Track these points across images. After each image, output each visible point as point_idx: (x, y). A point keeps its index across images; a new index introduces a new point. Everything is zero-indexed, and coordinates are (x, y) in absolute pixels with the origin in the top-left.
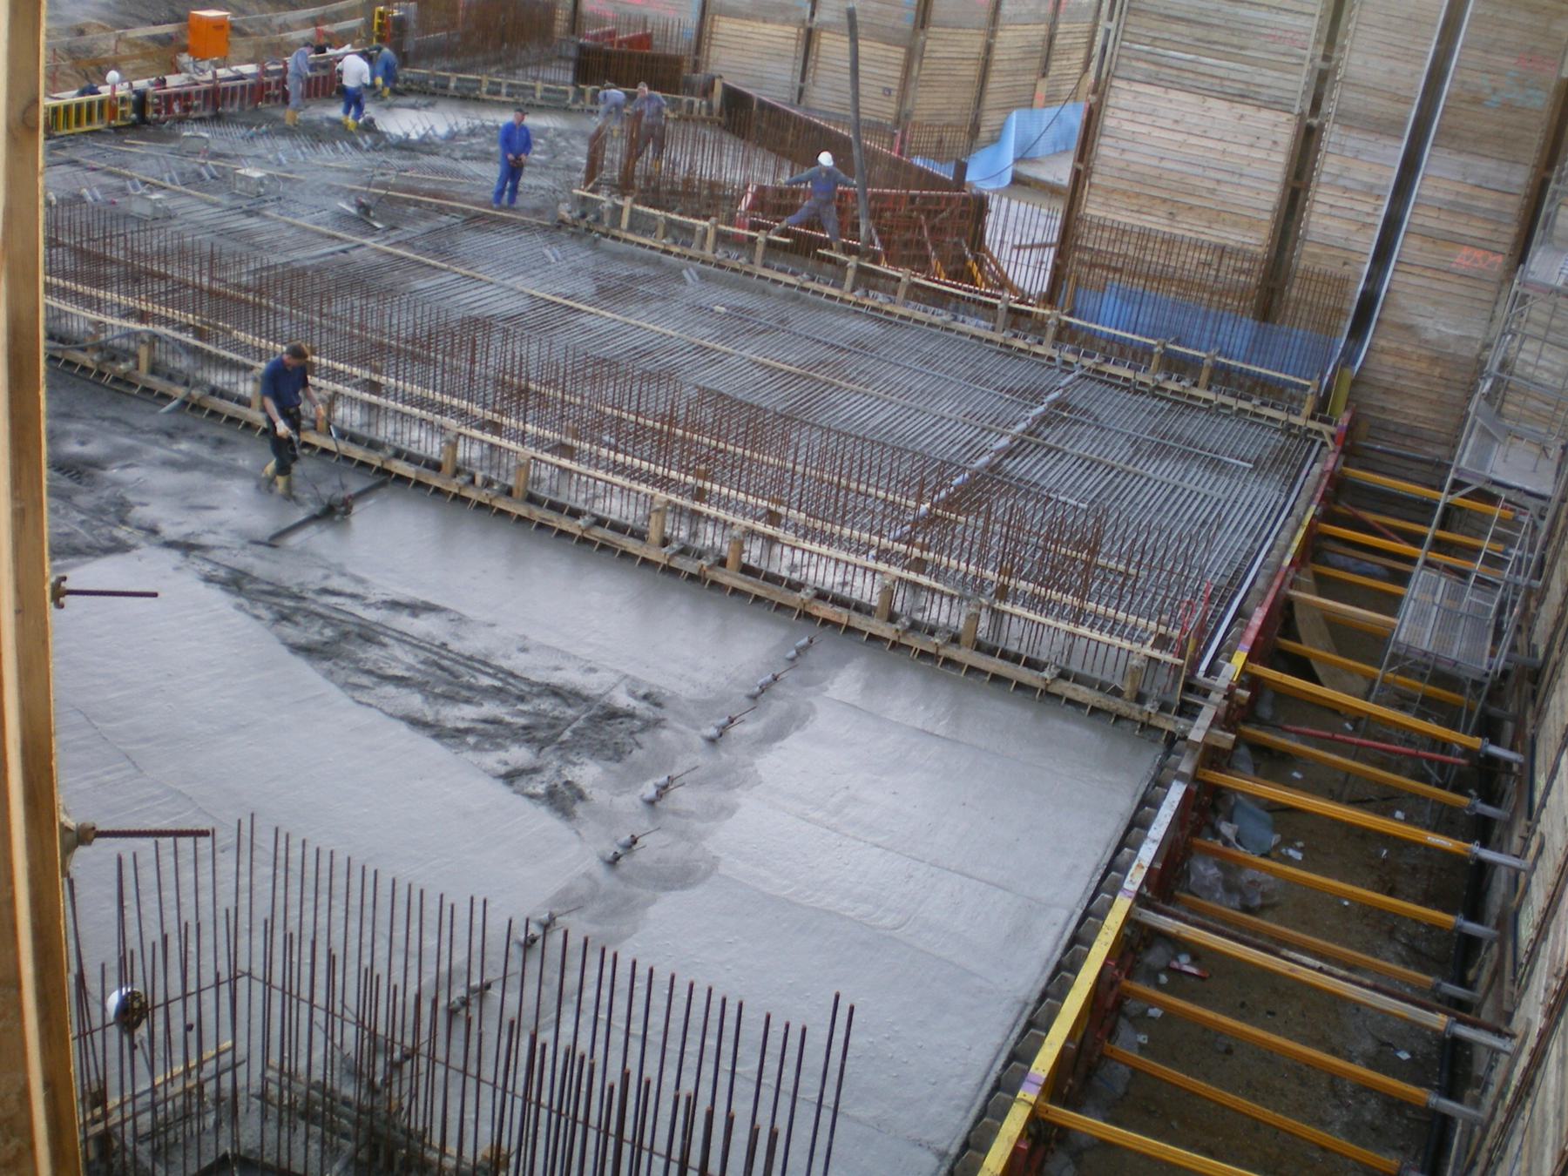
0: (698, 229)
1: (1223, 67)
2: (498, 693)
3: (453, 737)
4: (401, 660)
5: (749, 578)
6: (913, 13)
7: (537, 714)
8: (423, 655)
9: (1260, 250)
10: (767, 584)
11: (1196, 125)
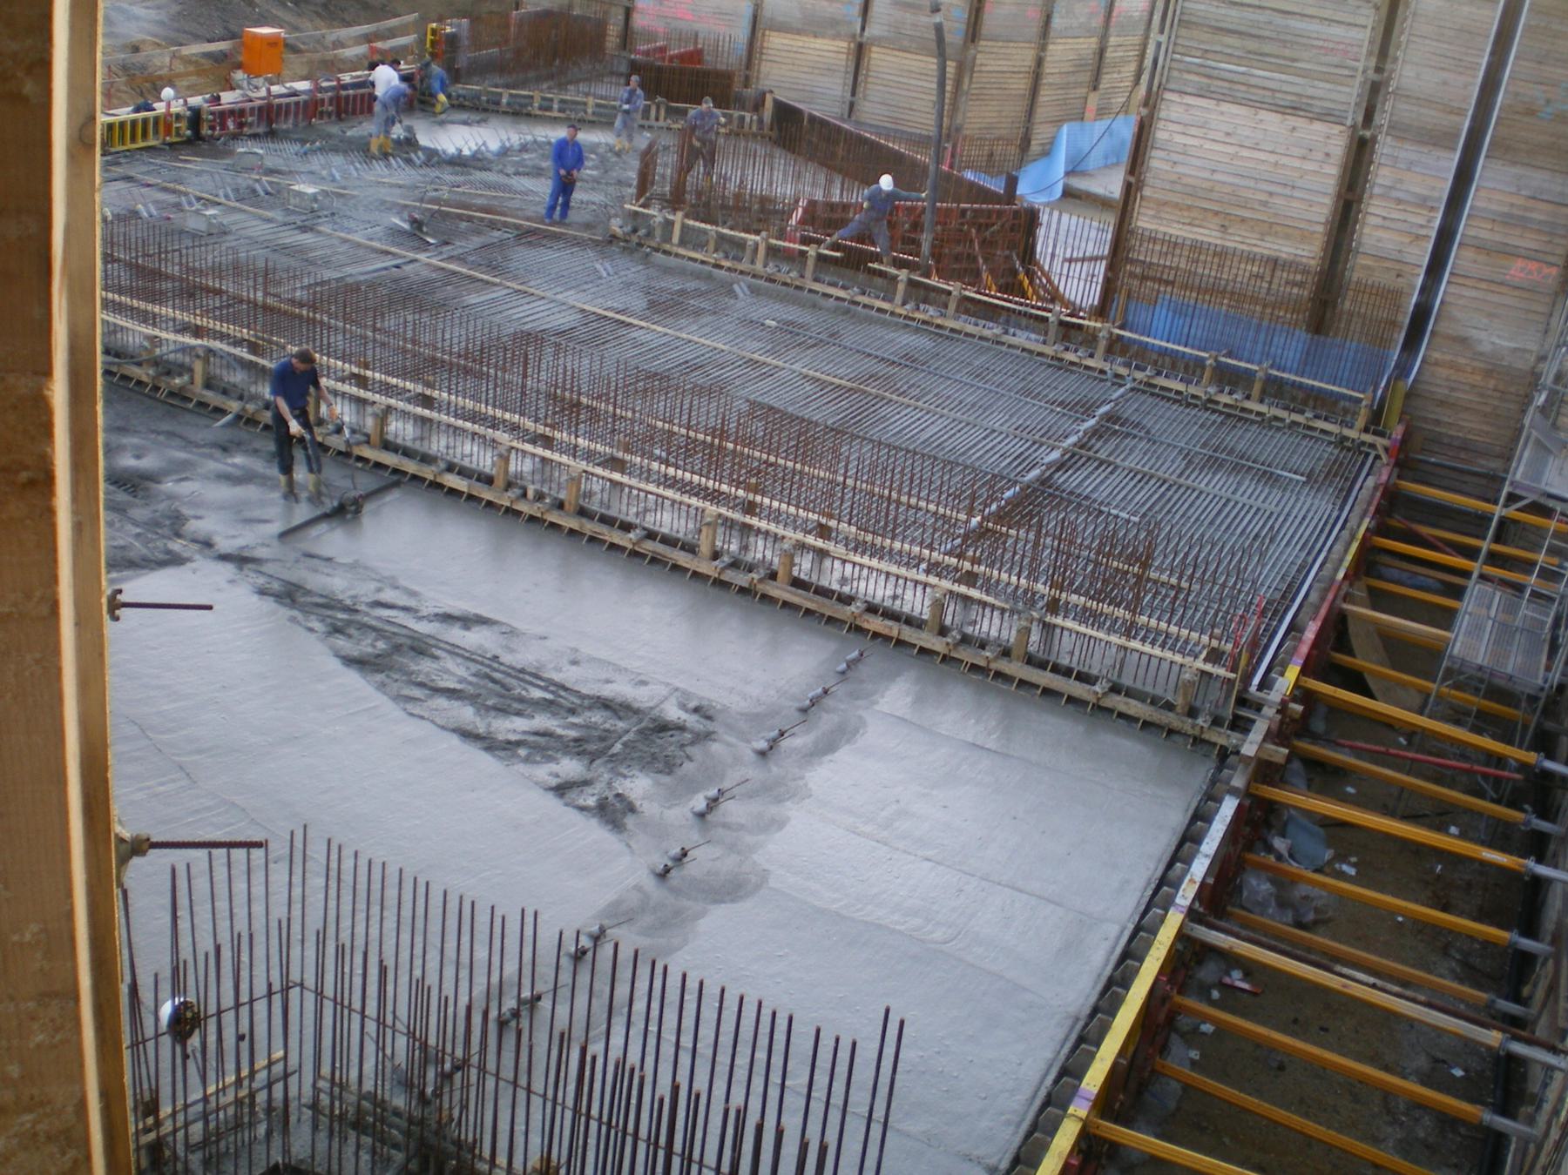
0: (750, 243)
2: (548, 706)
3: (505, 749)
4: (454, 672)
5: (800, 591)
6: (963, 27)
7: (587, 727)
8: (474, 667)
9: (1313, 262)
10: (817, 598)
11: (1247, 137)
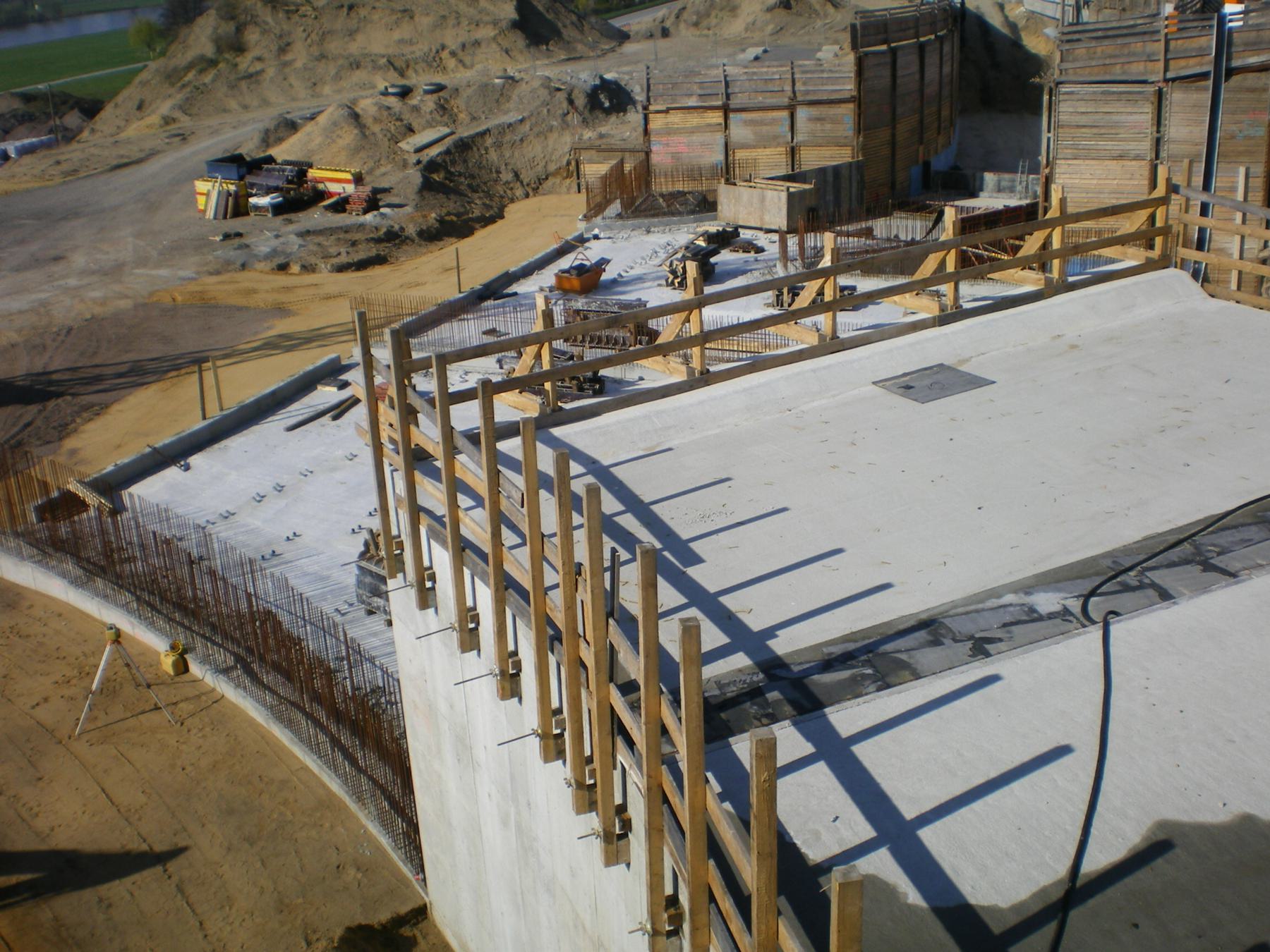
1: (1110, 145)
